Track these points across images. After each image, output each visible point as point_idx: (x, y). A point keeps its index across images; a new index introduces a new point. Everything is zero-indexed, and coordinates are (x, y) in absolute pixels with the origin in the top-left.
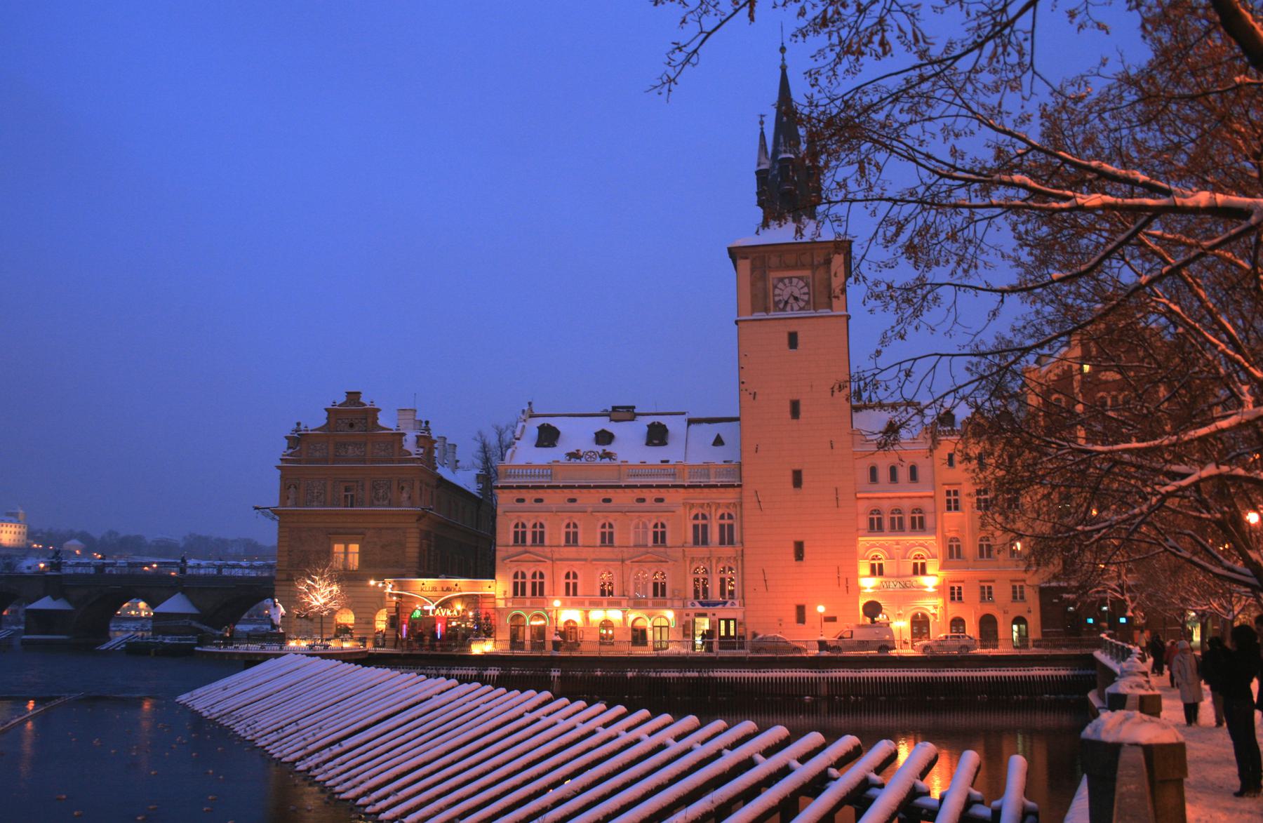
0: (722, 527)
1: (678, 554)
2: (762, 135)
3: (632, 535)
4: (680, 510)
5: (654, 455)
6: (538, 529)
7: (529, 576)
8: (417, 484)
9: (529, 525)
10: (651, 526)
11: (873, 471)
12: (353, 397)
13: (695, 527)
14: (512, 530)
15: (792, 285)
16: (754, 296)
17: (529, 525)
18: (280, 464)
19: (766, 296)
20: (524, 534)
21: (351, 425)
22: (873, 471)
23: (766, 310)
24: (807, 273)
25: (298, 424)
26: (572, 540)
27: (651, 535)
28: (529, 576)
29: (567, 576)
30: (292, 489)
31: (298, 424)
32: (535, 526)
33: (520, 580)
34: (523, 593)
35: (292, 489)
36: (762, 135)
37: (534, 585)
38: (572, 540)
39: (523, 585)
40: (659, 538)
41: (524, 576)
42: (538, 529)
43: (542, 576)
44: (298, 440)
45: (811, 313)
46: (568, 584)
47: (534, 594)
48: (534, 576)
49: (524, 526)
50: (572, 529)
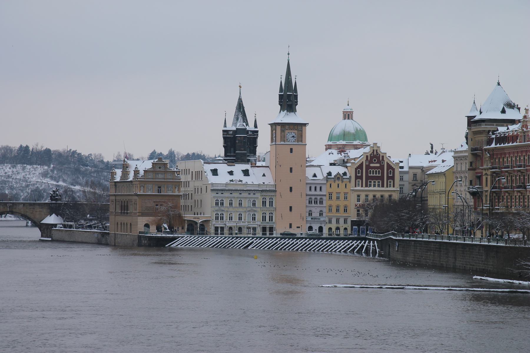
0: (270, 202)
1: (259, 210)
2: (281, 82)
4: (260, 197)
5: (245, 179)
9: (220, 201)
11: (310, 188)
15: (290, 134)
16: (281, 137)
17: (220, 201)
19: (284, 137)
22: (310, 188)
23: (284, 141)
24: (296, 131)
26: (231, 204)
36: (281, 82)
38: (231, 204)
40: (254, 204)
45: (296, 143)
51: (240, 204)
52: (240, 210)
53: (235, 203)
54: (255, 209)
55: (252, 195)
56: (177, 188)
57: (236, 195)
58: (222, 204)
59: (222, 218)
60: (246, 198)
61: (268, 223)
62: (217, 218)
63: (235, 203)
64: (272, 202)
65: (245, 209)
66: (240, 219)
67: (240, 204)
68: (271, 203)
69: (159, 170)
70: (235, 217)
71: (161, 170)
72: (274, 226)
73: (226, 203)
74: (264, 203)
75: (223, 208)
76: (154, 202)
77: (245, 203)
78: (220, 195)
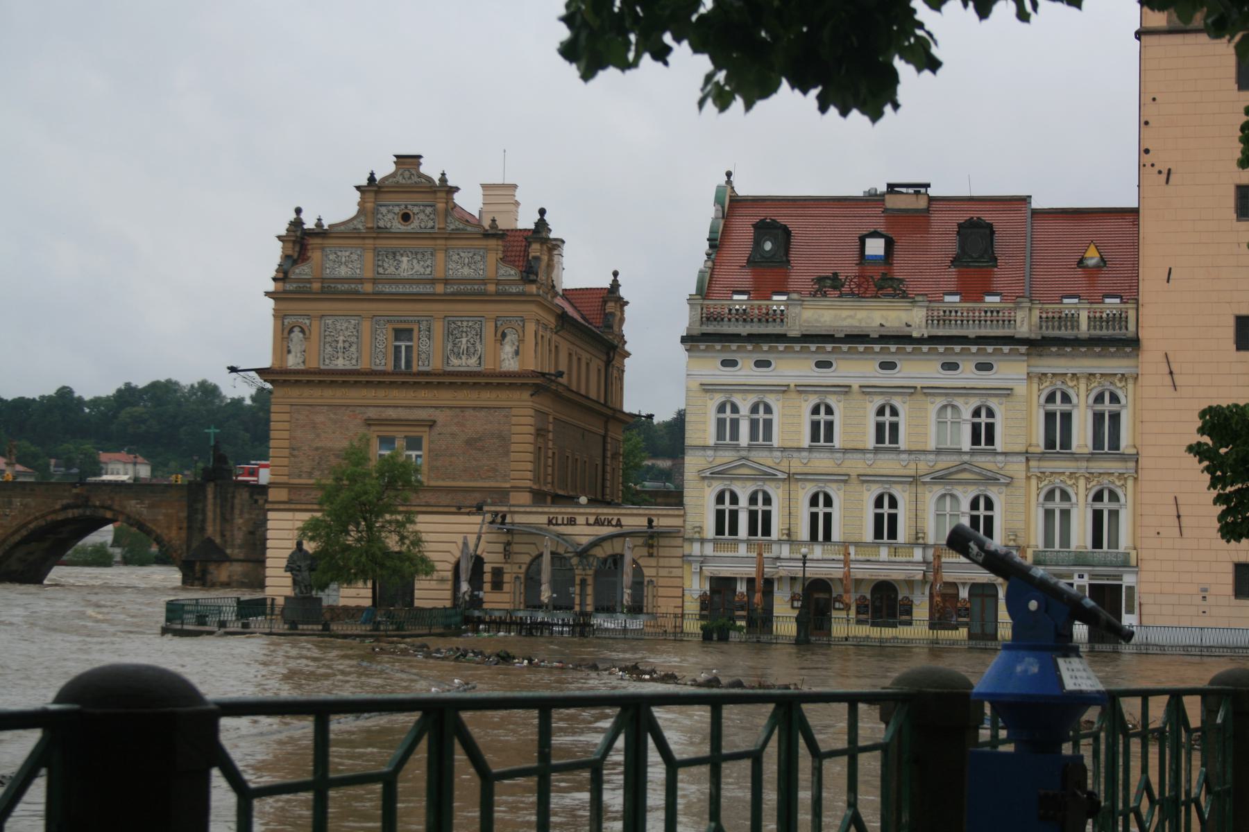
0: (1098, 418)
1: (1017, 468)
3: (932, 429)
6: (761, 415)
7: (743, 502)
8: (531, 327)
9: (744, 409)
10: (967, 414)
12: (408, 162)
13: (1050, 417)
14: (712, 417)
17: (744, 409)
18: (271, 287)
20: (735, 424)
21: (406, 217)
25: (298, 211)
26: (822, 432)
27: (967, 431)
28: (743, 502)
29: (814, 501)
30: (297, 335)
31: (298, 211)
32: (755, 409)
33: (727, 506)
34: (734, 530)
35: (297, 335)
37: (753, 515)
38: (822, 432)
39: (734, 515)
40: (983, 434)
41: (734, 499)
42: (761, 415)
43: (767, 500)
44: (301, 240)
46: (814, 517)
47: (752, 531)
48: (753, 500)
49: (735, 409)
50: (822, 417)
51: (887, 433)
52: (887, 464)
53: (855, 424)
54: (983, 462)
55: (967, 374)
56: (511, 337)
57: (856, 370)
58: (762, 429)
59: (761, 524)
60: (929, 391)
61: (1080, 560)
62: (725, 523)
63: (855, 424)
64: (1115, 417)
65: (923, 466)
66: (885, 527)
67: (887, 433)
68: (1107, 428)
69: (398, 226)
70: (853, 516)
71: (414, 225)
72: (1128, 580)
73: (790, 423)
74: (1057, 430)
75: (763, 459)
76: (369, 423)
77: (922, 427)
78: (746, 372)
